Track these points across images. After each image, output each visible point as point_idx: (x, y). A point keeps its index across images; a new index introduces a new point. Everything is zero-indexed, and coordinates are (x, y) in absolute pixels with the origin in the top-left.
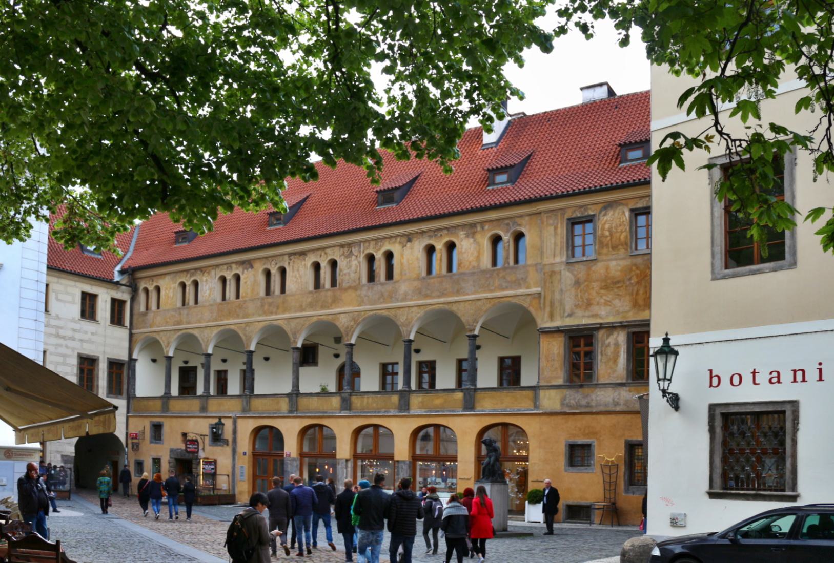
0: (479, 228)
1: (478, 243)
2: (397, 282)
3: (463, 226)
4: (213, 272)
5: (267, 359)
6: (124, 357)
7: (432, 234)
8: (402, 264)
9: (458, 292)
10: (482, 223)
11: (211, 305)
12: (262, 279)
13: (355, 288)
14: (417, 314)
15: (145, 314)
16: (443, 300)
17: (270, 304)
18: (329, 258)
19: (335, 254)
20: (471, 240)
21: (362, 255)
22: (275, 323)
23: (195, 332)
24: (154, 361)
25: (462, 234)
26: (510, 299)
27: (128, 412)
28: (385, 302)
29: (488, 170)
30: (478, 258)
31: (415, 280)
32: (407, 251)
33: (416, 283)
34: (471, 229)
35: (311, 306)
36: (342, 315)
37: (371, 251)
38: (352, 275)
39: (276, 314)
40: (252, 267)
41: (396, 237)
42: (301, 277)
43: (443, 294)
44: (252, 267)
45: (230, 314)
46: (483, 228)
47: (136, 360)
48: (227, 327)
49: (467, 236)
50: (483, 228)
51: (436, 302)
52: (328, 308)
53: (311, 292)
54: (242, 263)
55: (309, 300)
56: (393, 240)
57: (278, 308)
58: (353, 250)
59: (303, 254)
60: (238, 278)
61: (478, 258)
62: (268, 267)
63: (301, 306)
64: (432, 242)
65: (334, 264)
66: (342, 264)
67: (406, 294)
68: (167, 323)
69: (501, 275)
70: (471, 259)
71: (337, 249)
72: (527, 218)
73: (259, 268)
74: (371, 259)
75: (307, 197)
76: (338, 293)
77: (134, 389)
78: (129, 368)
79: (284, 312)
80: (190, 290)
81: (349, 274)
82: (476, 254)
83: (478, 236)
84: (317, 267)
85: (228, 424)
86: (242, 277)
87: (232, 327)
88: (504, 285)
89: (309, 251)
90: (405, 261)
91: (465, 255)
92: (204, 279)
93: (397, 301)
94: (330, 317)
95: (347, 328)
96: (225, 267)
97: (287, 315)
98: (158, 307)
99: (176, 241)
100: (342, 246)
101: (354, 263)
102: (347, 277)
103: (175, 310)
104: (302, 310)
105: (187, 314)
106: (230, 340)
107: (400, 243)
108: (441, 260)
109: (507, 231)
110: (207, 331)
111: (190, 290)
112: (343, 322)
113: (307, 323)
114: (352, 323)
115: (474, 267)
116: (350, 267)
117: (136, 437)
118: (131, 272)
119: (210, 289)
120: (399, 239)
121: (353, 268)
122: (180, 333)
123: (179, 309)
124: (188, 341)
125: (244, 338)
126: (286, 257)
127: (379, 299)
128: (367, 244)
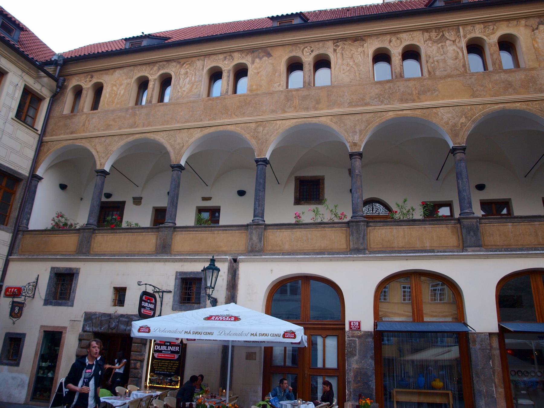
11: (194, 102)
23: (161, 138)
35: (380, 98)
38: (450, 62)
39: (316, 109)
42: (357, 65)
52: (414, 101)
55: (377, 91)
57: (318, 102)
58: (447, 35)
63: (363, 100)
68: (108, 127)
77: (28, 220)
81: (444, 61)
92: (183, 71)
94: (418, 113)
98: (95, 106)
102: (441, 64)
103: (127, 110)
104: (366, 104)
107: (526, 25)
110: (184, 135)
111: (154, 86)
123: (132, 108)
128: (469, 28)
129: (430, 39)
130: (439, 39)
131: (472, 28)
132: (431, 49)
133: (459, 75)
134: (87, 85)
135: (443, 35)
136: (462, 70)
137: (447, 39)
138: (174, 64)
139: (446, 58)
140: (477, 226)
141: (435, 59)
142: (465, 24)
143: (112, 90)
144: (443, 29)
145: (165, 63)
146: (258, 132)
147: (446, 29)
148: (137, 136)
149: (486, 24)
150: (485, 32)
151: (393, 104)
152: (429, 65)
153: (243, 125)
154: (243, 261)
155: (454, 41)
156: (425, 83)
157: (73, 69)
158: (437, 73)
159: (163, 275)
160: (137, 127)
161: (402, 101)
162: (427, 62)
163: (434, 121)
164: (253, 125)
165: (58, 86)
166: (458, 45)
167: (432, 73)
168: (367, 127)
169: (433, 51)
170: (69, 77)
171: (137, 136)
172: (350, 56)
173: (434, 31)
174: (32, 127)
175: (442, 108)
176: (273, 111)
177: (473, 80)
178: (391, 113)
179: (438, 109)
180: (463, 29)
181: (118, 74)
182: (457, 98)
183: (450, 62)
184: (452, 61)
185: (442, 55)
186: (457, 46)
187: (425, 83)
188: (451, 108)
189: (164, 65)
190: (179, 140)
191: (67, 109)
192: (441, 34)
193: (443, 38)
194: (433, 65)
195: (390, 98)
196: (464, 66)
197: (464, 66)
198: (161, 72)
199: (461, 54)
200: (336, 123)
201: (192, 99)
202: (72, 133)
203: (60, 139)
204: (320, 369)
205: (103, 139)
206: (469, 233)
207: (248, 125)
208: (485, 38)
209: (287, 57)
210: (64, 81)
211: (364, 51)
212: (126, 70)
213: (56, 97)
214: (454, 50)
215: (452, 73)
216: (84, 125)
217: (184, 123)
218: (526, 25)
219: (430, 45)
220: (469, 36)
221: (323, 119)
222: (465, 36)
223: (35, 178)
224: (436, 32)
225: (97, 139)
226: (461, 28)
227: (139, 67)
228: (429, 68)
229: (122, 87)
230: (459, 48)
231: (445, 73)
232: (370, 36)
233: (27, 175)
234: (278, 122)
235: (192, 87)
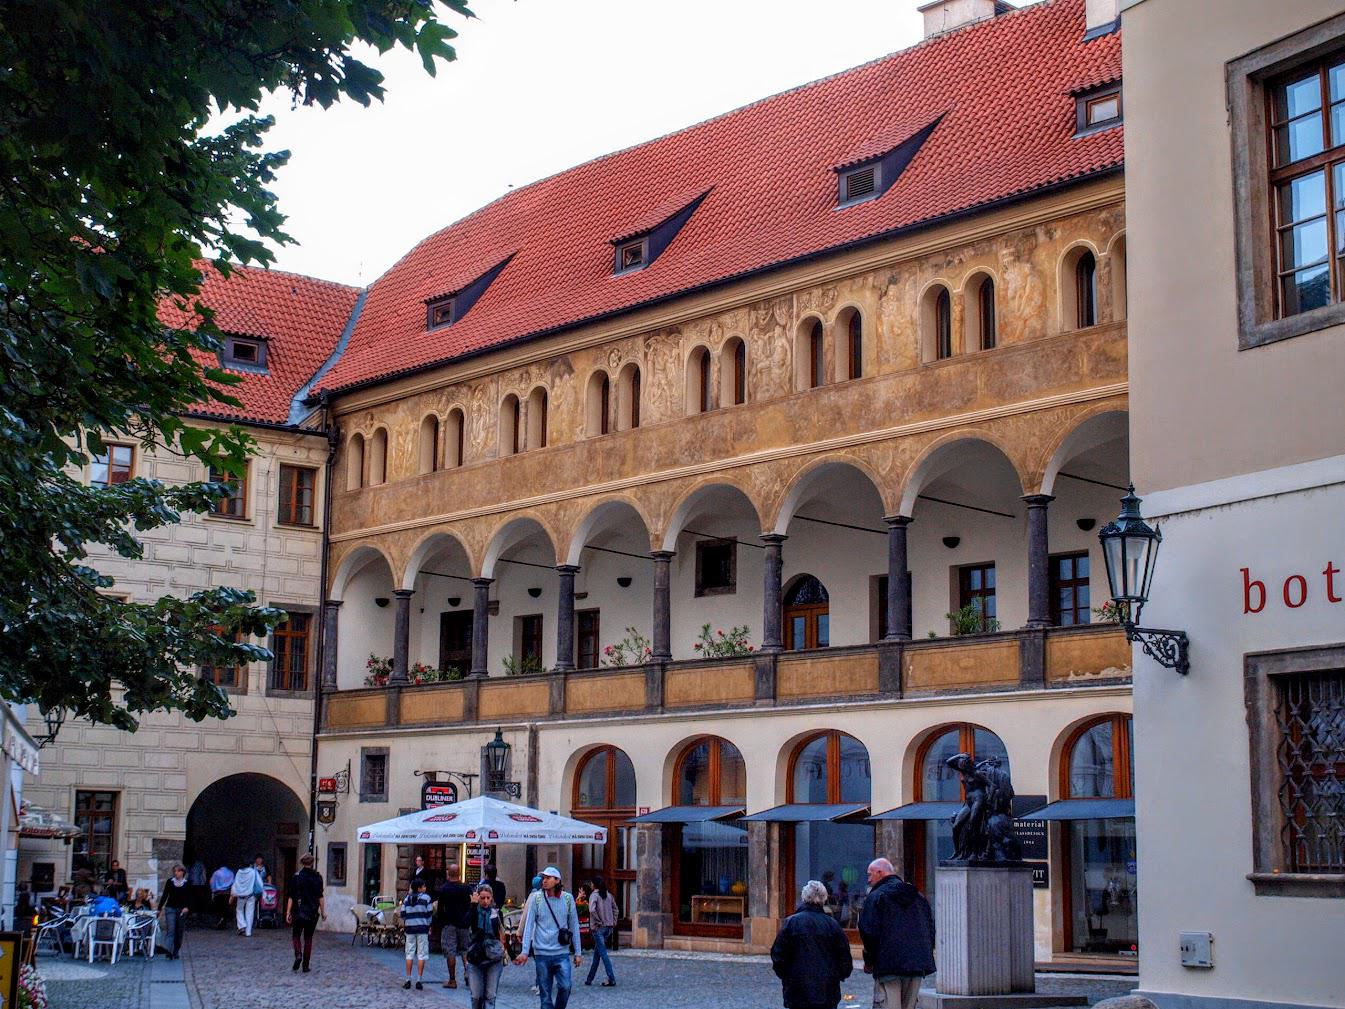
0: (1042, 238)
2: (871, 380)
4: (492, 388)
5: (625, 582)
6: (308, 595)
7: (940, 259)
8: (879, 337)
9: (1001, 396)
10: (1047, 223)
11: (489, 465)
12: (588, 395)
14: (915, 453)
15: (355, 496)
16: (967, 416)
17: (609, 453)
18: (729, 335)
19: (739, 325)
20: (1027, 268)
21: (796, 324)
22: (617, 496)
23: (457, 531)
24: (382, 603)
25: (1005, 253)
27: (317, 730)
28: (846, 432)
29: (1073, 94)
30: (1043, 310)
32: (890, 306)
33: (911, 381)
34: (1025, 243)
35: (694, 450)
36: (756, 469)
37: (814, 312)
38: (776, 371)
39: (621, 475)
40: (571, 370)
41: (863, 274)
42: (670, 384)
43: (967, 403)
44: (571, 370)
45: (524, 484)
46: (1049, 234)
47: (339, 604)
48: (520, 514)
49: (1017, 257)
50: (1049, 234)
51: (955, 422)
52: (728, 454)
53: (691, 420)
54: (549, 362)
56: (859, 281)
59: (673, 330)
60: (541, 396)
61: (1043, 310)
62: (601, 366)
63: (673, 453)
64: (943, 279)
65: (737, 348)
66: (754, 348)
67: (889, 407)
70: (1028, 310)
71: (742, 313)
73: (585, 368)
74: (814, 330)
75: (704, 195)
76: (746, 416)
78: (322, 625)
79: (635, 471)
80: (447, 432)
81: (769, 368)
82: (1037, 299)
83: (1041, 255)
84: (703, 357)
85: (519, 741)
86: (551, 395)
87: (531, 513)
89: (686, 323)
90: (884, 329)
91: (1014, 304)
92: (475, 404)
93: (874, 424)
94: (729, 475)
95: (767, 498)
96: (516, 374)
97: (643, 476)
99: (432, 323)
100: (753, 306)
101: (780, 342)
102: (765, 378)
105: (441, 490)
106: (526, 543)
108: (962, 320)
113: (686, 493)
115: (1033, 331)
116: (771, 355)
117: (331, 786)
118: (328, 402)
119: (487, 429)
121: (777, 356)
122: (428, 533)
123: (425, 477)
124: (443, 555)
125: (554, 537)
126: (640, 341)
127: (833, 421)
128: (805, 297)
130: (768, 324)
133: (782, 399)
134: (369, 435)
135: (773, 315)
136: (786, 387)
137: (777, 324)
138: (464, 390)
142: (800, 290)
143: (398, 443)
145: (454, 388)
146: (559, 520)
148: (433, 530)
149: (825, 288)
150: (823, 304)
151: (704, 462)
153: (543, 507)
154: (543, 728)
155: (784, 327)
157: (347, 405)
159: (459, 754)
160: (432, 513)
161: (717, 453)
164: (553, 507)
165: (331, 445)
170: (345, 417)
171: (433, 530)
174: (311, 526)
176: (575, 481)
177: (796, 407)
178: (700, 479)
181: (402, 410)
182: (776, 446)
184: (777, 371)
185: (767, 357)
189: (453, 393)
190: (478, 538)
191: (352, 484)
193: (772, 322)
196: (790, 379)
197: (790, 379)
198: (451, 407)
200: (640, 499)
201: (489, 460)
202: (361, 526)
203: (349, 536)
204: (587, 870)
205: (396, 536)
207: (549, 506)
208: (822, 318)
209: (590, 373)
210: (338, 429)
212: (410, 403)
213: (333, 462)
214: (782, 346)
216: (373, 511)
217: (481, 506)
218: (874, 286)
221: (627, 493)
223: (329, 606)
225: (390, 536)
227: (424, 398)
229: (409, 438)
232: (686, 323)
233: (318, 604)
234: (580, 501)
235: (487, 438)
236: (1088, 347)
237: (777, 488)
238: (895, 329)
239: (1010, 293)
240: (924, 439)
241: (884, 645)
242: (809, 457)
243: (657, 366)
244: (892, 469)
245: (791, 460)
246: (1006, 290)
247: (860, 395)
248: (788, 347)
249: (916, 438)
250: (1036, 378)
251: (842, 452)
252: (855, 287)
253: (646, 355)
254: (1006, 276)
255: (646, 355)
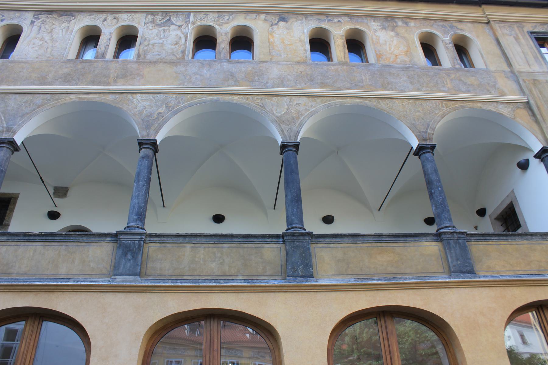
1: (404, 38)
3: (376, 17)
7: (325, 18)
9: (384, 87)
13: (174, 63)
20: (392, 33)
26: (479, 105)
30: (408, 52)
31: (298, 63)
33: (301, 68)
35: (67, 79)
42: (53, 40)
43: (356, 86)
49: (385, 28)
56: (254, 16)
58: (174, 19)
69: (453, 76)
70: (396, 52)
72: (469, 25)
81: (162, 45)
82: (403, 48)
88: (464, 88)
93: (265, 85)
102: (156, 48)
109: (445, 33)
112: (137, 108)
114: (162, 110)
120: (263, 16)
128: (202, 15)
129: (153, 21)
130: (163, 23)
131: (205, 16)
132: (150, 32)
135: (169, 20)
136: (179, 55)
137: (173, 24)
139: (165, 42)
140: (140, 245)
141: (151, 42)
144: (171, 14)
147: (175, 14)
152: (142, 47)
156: (129, 66)
158: (149, 57)
161: (93, 83)
162: (140, 44)
163: (125, 108)
166: (183, 30)
167: (142, 57)
168: (34, 110)
169: (152, 34)
172: (49, 31)
173: (160, 14)
175: (140, 95)
179: (134, 95)
180: (194, 16)
183: (168, 47)
184: (170, 46)
185: (161, 39)
186: (181, 31)
187: (129, 66)
188: (151, 95)
192: (168, 18)
194: (146, 48)
195: (79, 79)
196: (183, 52)
199: (183, 40)
206: (126, 255)
208: (217, 27)
211: (69, 27)
215: (167, 58)
219: (151, 28)
220: (199, 23)
222: (194, 23)
224: (162, 16)
226: (192, 15)
228: (141, 50)
230: (183, 34)
231: (158, 57)
236: (448, 75)
237: (160, 110)
238: (286, 42)
239: (381, 41)
240: (319, 100)
241: (293, 235)
242: (199, 96)
243: (43, 29)
244: (286, 113)
245: (179, 95)
246: (379, 39)
247: (253, 68)
248: (182, 36)
249: (311, 99)
250: (411, 83)
251: (235, 97)
252: (248, 17)
253: (32, 22)
254: (377, 34)
255: (32, 22)
